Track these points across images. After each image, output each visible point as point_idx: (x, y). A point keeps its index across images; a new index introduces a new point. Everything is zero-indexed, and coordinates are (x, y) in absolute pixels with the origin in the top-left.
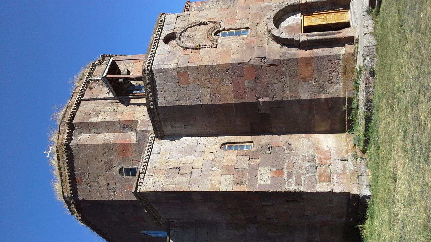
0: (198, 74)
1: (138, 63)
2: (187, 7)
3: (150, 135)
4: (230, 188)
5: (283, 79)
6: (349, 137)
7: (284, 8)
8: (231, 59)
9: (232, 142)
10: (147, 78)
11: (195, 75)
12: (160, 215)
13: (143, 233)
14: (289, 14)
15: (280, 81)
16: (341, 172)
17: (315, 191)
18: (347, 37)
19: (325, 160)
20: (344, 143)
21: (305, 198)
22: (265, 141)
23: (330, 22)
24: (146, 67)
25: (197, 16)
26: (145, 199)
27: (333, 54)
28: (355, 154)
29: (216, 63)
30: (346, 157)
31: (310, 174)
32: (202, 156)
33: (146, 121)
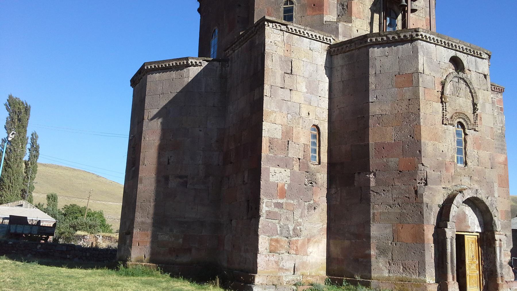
0: (409, 100)
1: (425, 23)
2: (496, 88)
3: (333, 39)
4: (266, 134)
5: (398, 205)
6: (322, 279)
7: (490, 211)
8: (427, 142)
9: (320, 138)
10: (406, 35)
11: (408, 95)
12: (237, 49)
13: (215, 30)
14: (482, 217)
15: (394, 201)
16: (281, 266)
17: (259, 234)
18: (447, 287)
19: (295, 248)
20: (314, 273)
21: (252, 221)
22: (320, 178)
23: (467, 268)
24: (421, 33)
25: (484, 100)
26: (257, 32)
27: (426, 268)
28: (301, 284)
29: (422, 122)
30: (298, 273)
31: (279, 229)
32: (305, 102)
33: (350, 33)
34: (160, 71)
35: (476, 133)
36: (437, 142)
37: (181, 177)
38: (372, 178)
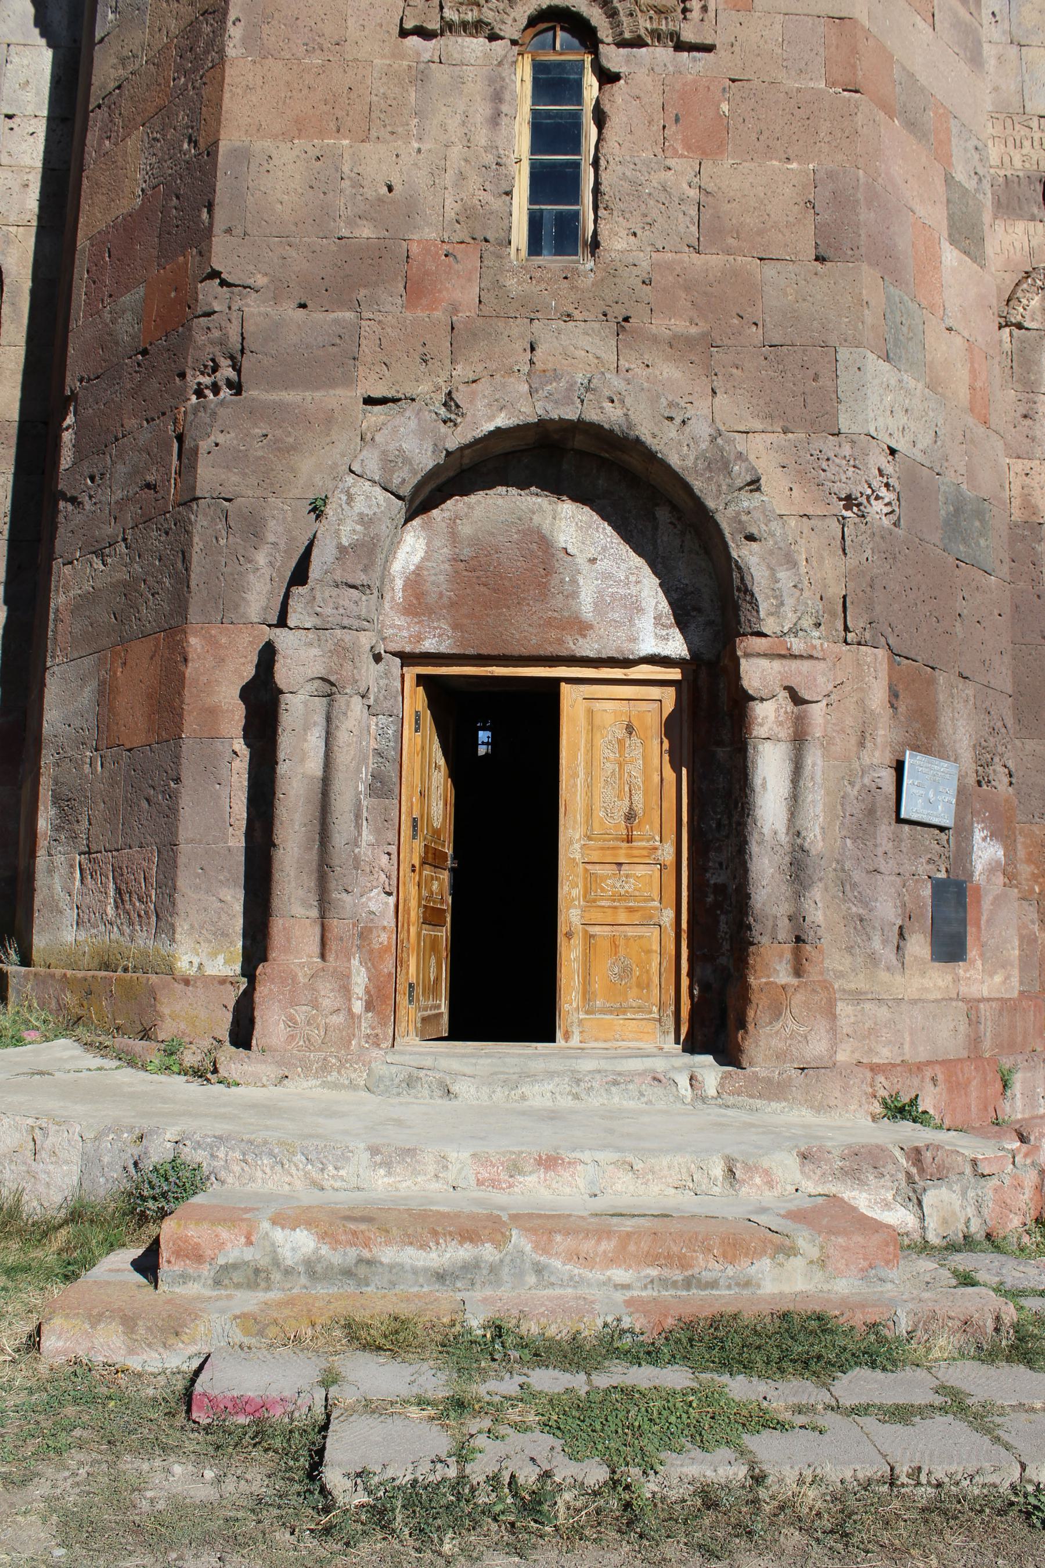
8: (261, 145)
27: (180, 883)
35: (695, 60)
36: (346, 142)
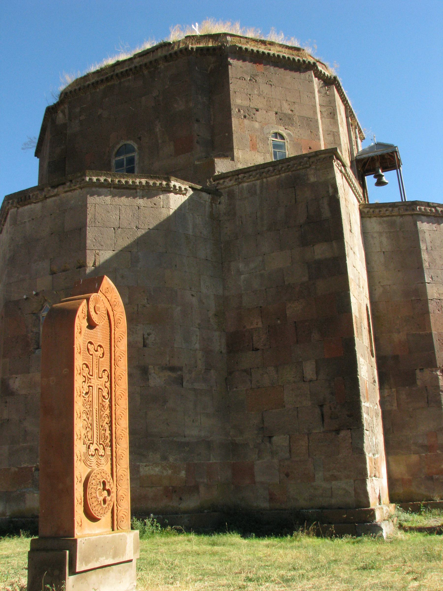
12: (248, 182)
26: (310, 166)
34: (112, 189)
37: (172, 369)
38: (439, 375)
